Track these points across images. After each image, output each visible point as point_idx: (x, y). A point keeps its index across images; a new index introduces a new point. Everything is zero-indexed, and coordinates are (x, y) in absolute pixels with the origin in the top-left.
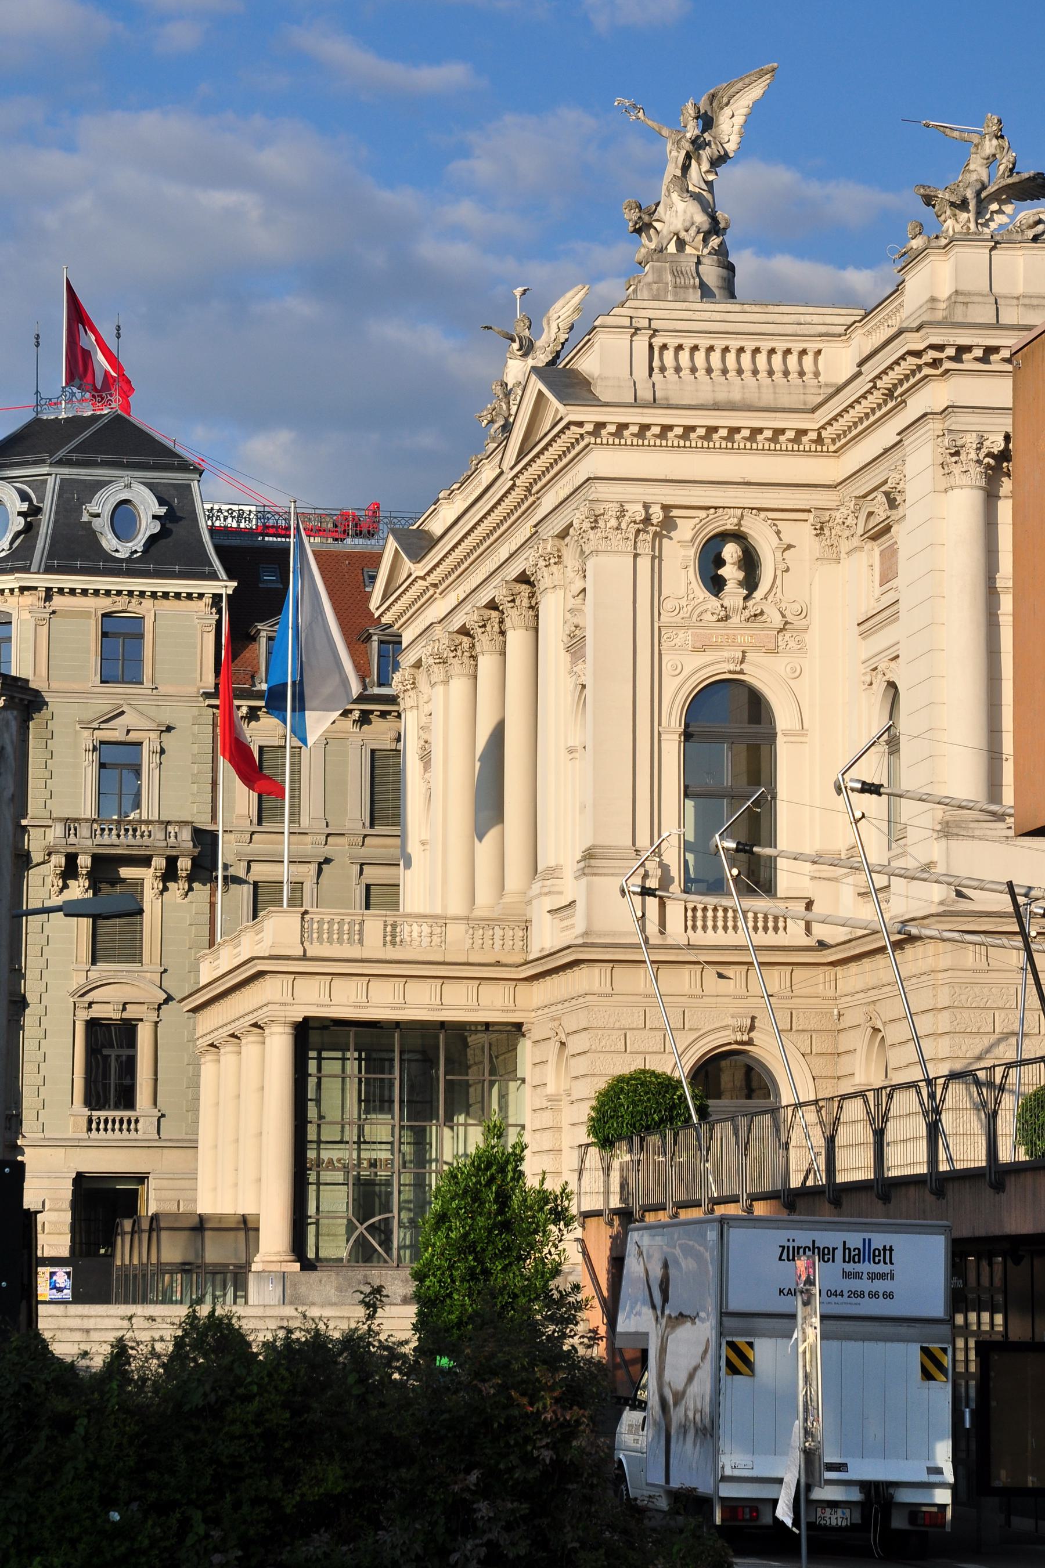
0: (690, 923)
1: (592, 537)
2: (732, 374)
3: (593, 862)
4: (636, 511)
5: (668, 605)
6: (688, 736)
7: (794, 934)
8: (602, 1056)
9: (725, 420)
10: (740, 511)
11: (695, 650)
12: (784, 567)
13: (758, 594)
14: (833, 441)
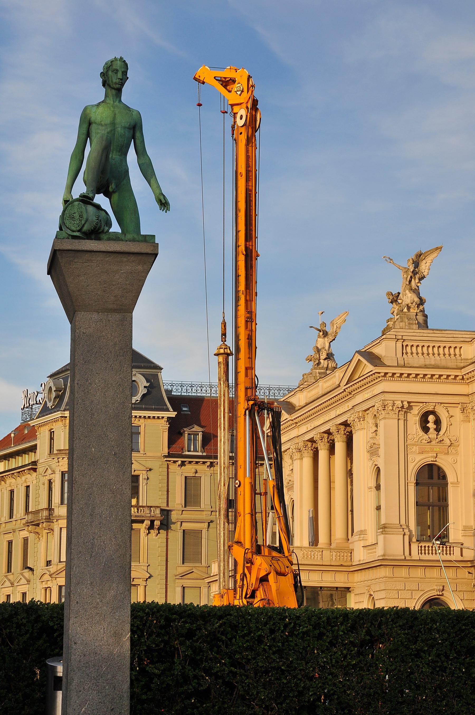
0: (420, 552)
1: (383, 413)
2: (431, 355)
3: (386, 529)
4: (399, 404)
5: (409, 437)
6: (417, 484)
7: (456, 555)
8: (390, 600)
9: (429, 372)
12: (449, 423)
13: (441, 433)
14: (468, 379)
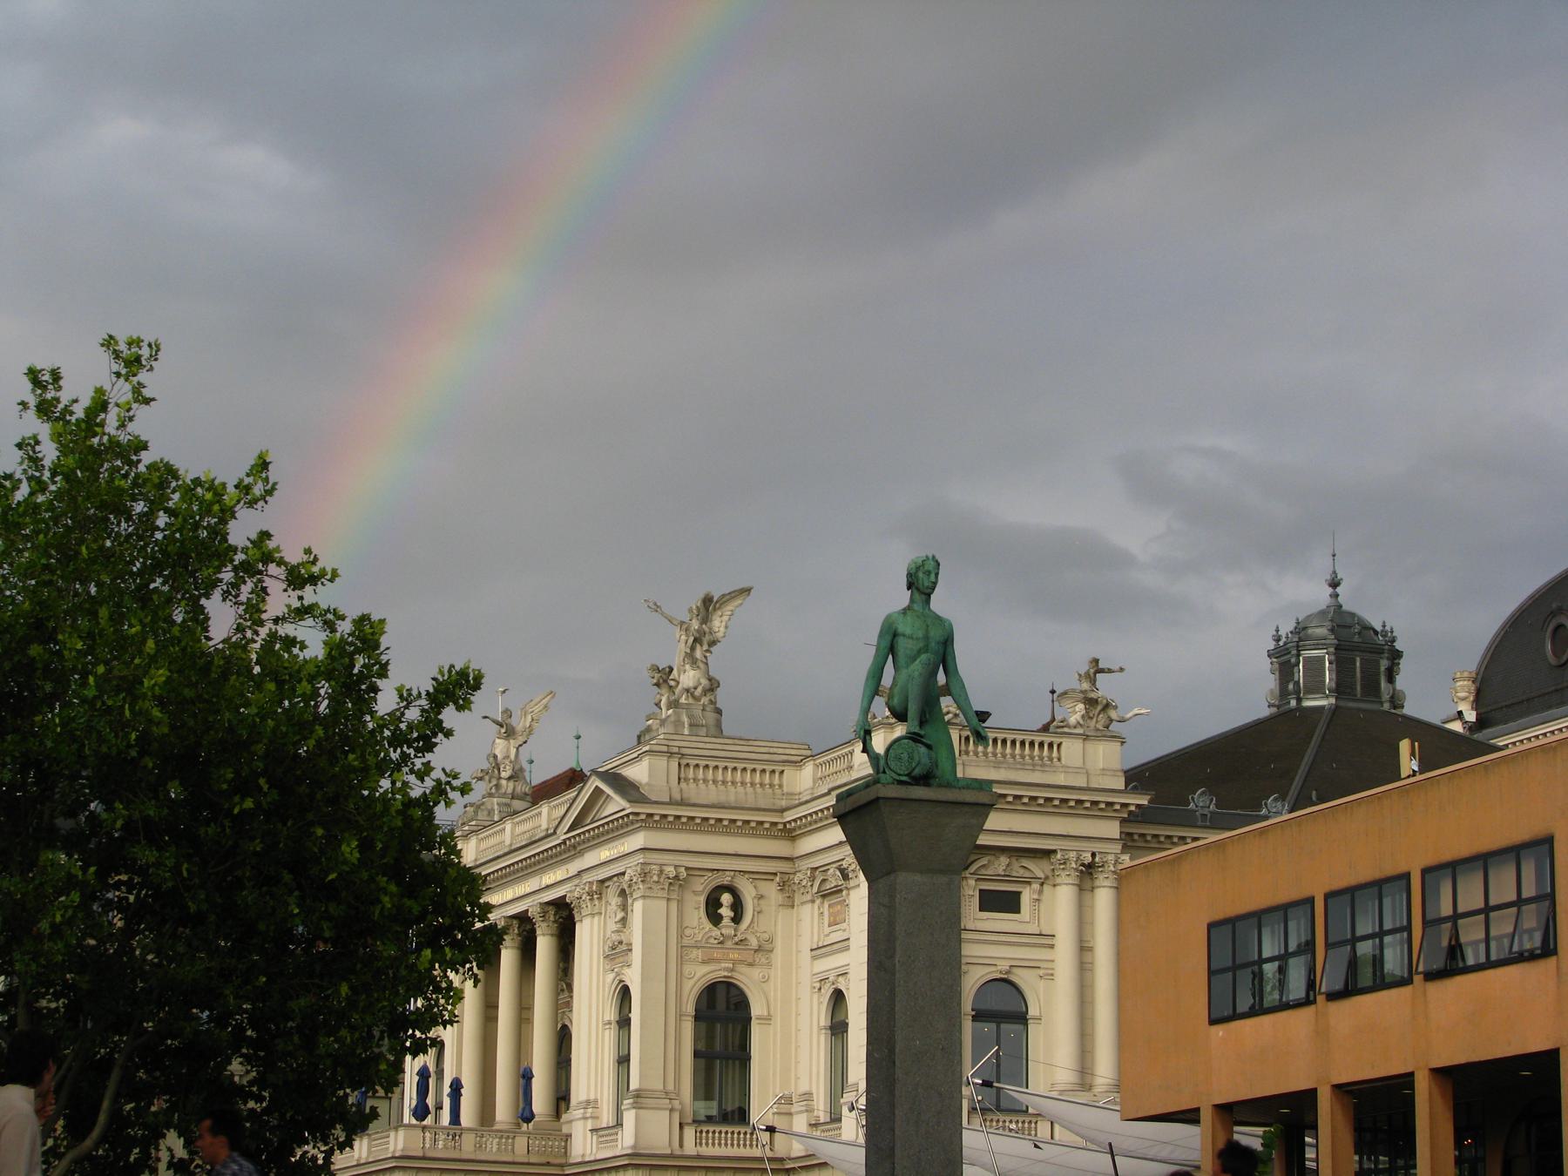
11: (704, 962)
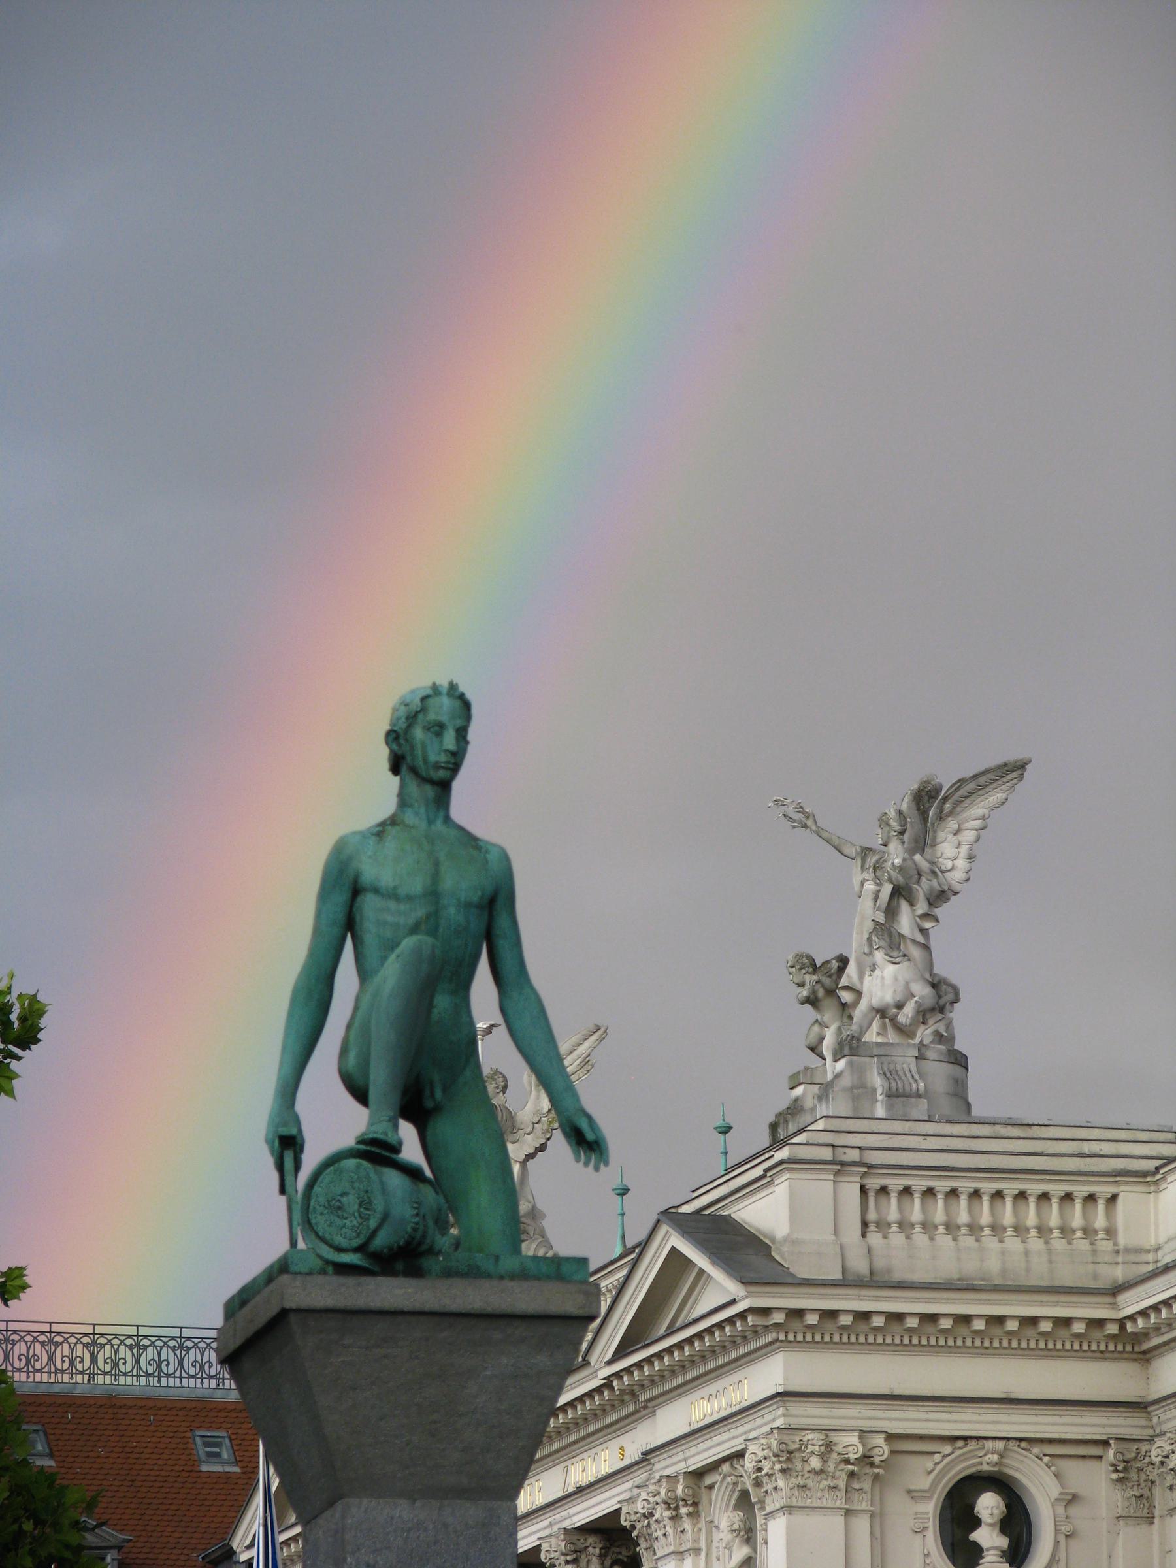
10: (1001, 1445)
